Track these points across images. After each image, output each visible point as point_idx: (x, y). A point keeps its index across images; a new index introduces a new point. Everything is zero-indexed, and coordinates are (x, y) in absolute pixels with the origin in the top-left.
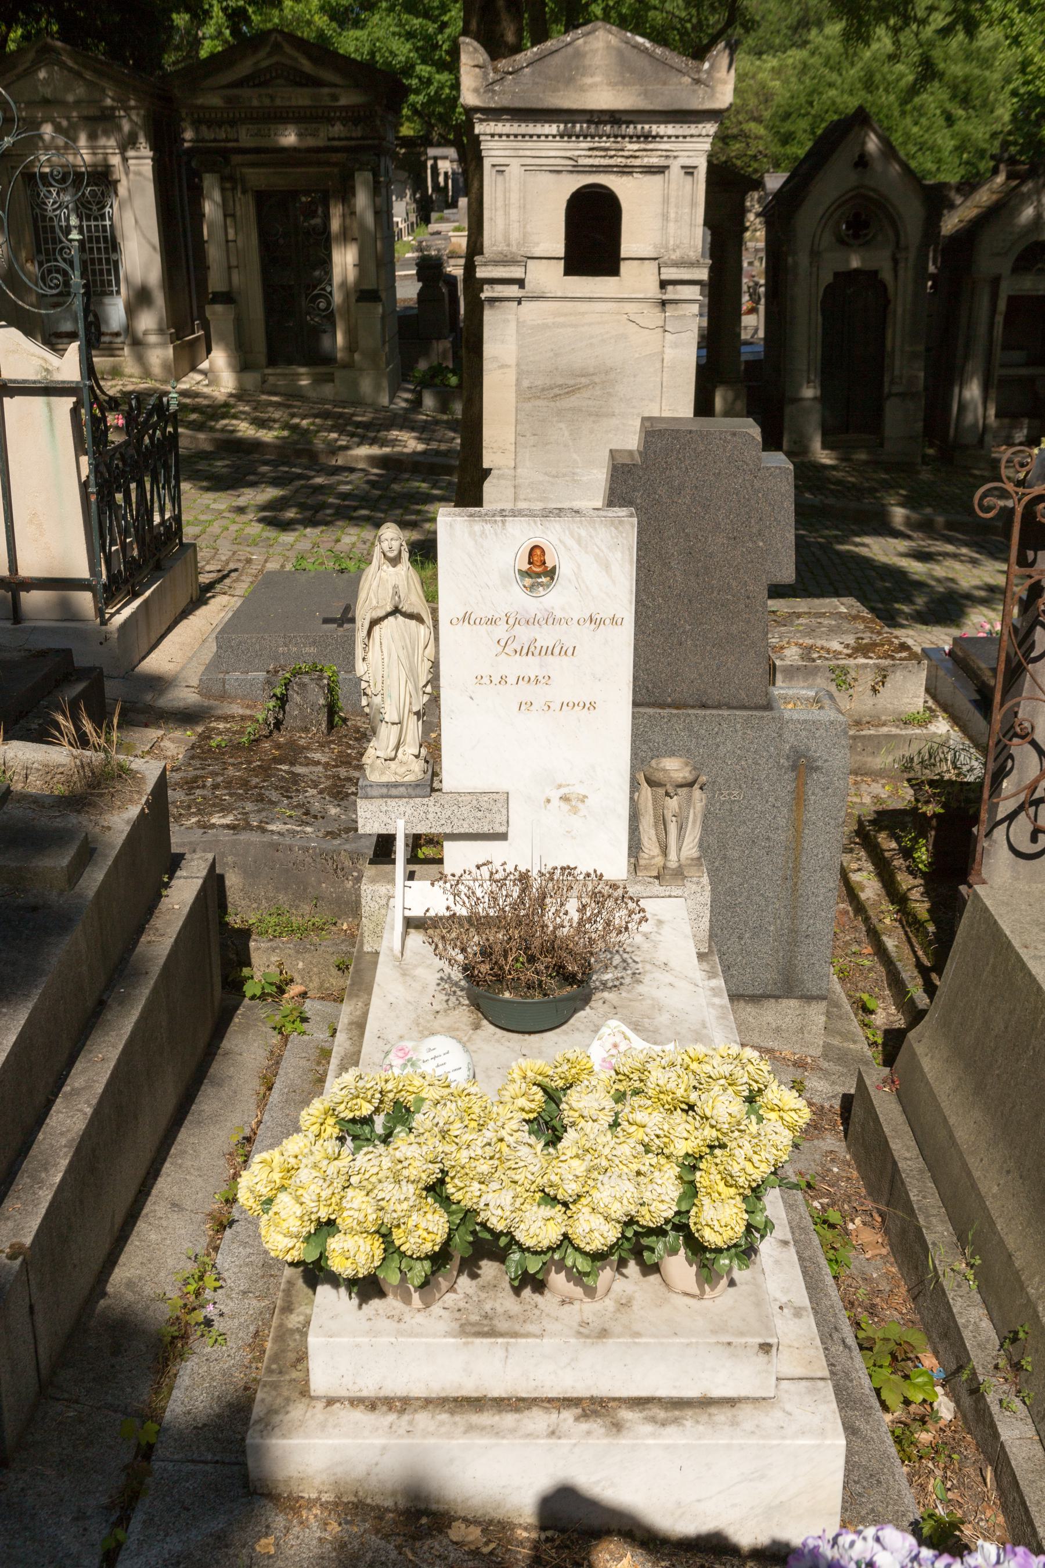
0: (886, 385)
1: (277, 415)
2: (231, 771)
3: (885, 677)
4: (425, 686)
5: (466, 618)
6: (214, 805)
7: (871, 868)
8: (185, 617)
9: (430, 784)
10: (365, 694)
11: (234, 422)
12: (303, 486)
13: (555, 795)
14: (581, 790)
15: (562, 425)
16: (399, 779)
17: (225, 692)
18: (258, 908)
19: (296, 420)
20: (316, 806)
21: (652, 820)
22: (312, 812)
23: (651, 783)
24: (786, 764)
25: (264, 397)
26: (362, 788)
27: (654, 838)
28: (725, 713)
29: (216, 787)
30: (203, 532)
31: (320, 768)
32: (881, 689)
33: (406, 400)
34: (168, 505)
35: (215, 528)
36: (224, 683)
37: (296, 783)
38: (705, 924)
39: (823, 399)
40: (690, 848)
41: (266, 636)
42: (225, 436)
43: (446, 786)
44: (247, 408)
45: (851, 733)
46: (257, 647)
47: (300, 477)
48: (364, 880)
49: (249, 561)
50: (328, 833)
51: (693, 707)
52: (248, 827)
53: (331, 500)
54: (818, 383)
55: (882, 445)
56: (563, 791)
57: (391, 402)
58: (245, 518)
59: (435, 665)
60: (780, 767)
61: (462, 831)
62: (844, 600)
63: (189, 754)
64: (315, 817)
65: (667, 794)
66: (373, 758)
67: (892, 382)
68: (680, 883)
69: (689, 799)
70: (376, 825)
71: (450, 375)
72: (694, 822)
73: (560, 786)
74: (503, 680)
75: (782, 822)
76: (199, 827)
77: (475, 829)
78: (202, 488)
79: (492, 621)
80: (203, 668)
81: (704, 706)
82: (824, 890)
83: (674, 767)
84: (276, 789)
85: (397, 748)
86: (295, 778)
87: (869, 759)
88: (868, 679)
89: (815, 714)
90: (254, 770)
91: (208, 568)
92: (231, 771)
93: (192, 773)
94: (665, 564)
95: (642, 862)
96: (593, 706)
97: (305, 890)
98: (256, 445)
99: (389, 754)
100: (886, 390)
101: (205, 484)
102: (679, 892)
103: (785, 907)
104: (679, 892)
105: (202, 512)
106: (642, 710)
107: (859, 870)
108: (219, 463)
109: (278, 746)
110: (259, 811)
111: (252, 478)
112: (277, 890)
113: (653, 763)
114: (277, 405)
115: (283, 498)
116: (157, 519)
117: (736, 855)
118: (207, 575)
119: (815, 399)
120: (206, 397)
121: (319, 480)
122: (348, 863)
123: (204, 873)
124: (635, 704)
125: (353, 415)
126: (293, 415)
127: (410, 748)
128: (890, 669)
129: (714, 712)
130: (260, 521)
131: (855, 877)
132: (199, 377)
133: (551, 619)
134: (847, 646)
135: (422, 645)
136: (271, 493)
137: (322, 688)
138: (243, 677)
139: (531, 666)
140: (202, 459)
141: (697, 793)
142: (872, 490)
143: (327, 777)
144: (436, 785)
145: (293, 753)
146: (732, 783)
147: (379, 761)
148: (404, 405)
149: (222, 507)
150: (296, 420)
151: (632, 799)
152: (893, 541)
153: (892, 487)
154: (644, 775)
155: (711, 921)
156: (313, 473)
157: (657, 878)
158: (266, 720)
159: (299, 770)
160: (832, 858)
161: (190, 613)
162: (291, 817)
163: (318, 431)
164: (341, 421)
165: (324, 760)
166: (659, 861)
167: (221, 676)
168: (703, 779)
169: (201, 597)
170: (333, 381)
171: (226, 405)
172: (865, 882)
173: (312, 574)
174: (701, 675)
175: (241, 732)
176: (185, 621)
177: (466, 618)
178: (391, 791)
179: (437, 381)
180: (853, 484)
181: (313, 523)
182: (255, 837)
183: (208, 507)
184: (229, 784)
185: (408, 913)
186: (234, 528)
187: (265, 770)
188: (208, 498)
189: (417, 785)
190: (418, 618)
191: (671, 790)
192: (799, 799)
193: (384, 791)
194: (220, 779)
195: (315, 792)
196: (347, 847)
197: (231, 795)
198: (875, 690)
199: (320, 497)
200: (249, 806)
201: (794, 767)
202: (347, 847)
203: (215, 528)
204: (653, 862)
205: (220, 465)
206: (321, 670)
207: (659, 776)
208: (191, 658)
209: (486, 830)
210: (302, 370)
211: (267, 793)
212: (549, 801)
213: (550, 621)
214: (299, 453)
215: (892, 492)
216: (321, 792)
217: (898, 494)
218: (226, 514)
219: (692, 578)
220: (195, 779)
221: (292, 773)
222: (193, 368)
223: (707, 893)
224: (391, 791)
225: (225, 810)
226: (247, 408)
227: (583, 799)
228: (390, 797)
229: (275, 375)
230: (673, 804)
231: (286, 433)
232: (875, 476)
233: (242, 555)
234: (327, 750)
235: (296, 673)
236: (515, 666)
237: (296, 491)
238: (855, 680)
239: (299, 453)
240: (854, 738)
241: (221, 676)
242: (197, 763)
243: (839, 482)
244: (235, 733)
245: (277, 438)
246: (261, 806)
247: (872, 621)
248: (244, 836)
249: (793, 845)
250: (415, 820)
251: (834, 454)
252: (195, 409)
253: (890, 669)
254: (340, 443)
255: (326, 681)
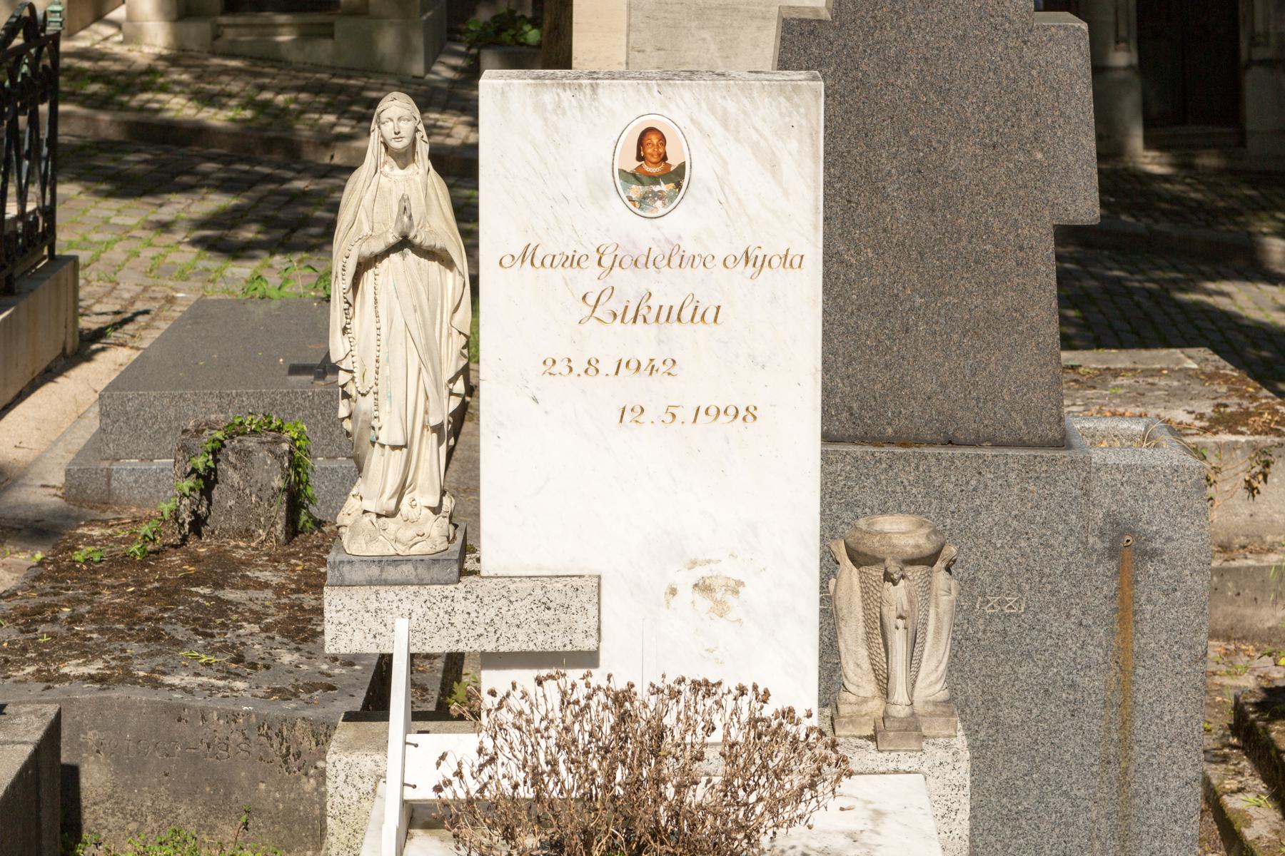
0: (1244, 44)
1: (235, 87)
2: (106, 596)
3: (1267, 465)
4: (453, 380)
5: (527, 256)
6: (70, 647)
7: (1261, 786)
8: (51, 380)
9: (461, 558)
10: (346, 396)
11: (162, 96)
12: (272, 193)
13: (684, 580)
14: (731, 570)
15: (706, 34)
16: (402, 550)
17: (110, 493)
18: (138, 832)
19: (267, 95)
20: (256, 650)
21: (861, 630)
22: (248, 658)
23: (859, 558)
24: (1099, 546)
25: (216, 61)
26: (335, 566)
27: (866, 665)
28: (989, 453)
29: (75, 619)
30: (96, 259)
31: (269, 594)
32: (1261, 486)
33: (454, 68)
34: (34, 190)
35: (117, 253)
36: (109, 477)
37: (222, 614)
38: (962, 824)
39: (1144, 67)
40: (931, 682)
41: (188, 394)
42: (144, 116)
43: (487, 567)
44: (185, 77)
45: (1215, 564)
46: (172, 413)
47: (267, 178)
48: (333, 746)
49: (171, 300)
50: (275, 691)
51: (931, 444)
52: (128, 678)
53: (318, 214)
54: (1133, 44)
55: (1242, 143)
56: (700, 572)
57: (428, 70)
58: (168, 239)
59: (471, 345)
60: (1089, 551)
61: (515, 647)
62: (1192, 351)
63: (33, 573)
64: (253, 666)
65: (888, 577)
66: (356, 513)
67: (1253, 43)
68: (914, 745)
69: (927, 588)
70: (358, 636)
71: (527, 28)
72: (938, 632)
73: (694, 564)
74: (592, 366)
75: (1096, 654)
76: (39, 680)
77: (540, 643)
78: (97, 193)
79: (573, 261)
80: (72, 456)
81: (950, 442)
82: (1175, 784)
83: (900, 531)
84: (185, 622)
85: (400, 493)
86: (222, 607)
87: (1249, 611)
88: (1239, 468)
89: (1148, 456)
90: (149, 593)
91: (97, 308)
92: (106, 596)
93: (35, 600)
94: (875, 191)
95: (845, 710)
96: (751, 414)
97: (227, 796)
98: (198, 132)
99: (385, 509)
100: (1244, 56)
101: (104, 187)
102: (912, 763)
103: (1108, 816)
104: (912, 763)
105: (97, 229)
106: (842, 448)
107: (1240, 790)
108: (131, 158)
109: (196, 560)
110: (151, 655)
111: (185, 179)
112: (177, 796)
113: (862, 523)
114: (235, 73)
115: (236, 209)
116: (12, 210)
117: (1017, 717)
118: (94, 318)
119: (1129, 67)
120: (116, 58)
121: (300, 184)
122: (308, 744)
123: (38, 736)
124: (827, 438)
125: (363, 88)
126: (262, 88)
127: (425, 494)
128: (1275, 452)
129: (970, 451)
130: (194, 243)
131: (1233, 803)
132: (107, 31)
133: (677, 258)
134: (1201, 417)
135: (449, 307)
136: (217, 202)
137: (278, 457)
138: (144, 466)
139: (642, 341)
140: (102, 150)
141: (940, 577)
142: (1231, 213)
143: (280, 608)
144: (469, 565)
145: (222, 570)
146: (1006, 581)
147: (366, 519)
148: (448, 74)
149: (131, 221)
150: (267, 95)
151: (823, 588)
152: (1268, 289)
153: (1264, 209)
154: (846, 548)
155: (973, 817)
156: (290, 174)
157: (873, 738)
158: (176, 515)
159: (228, 594)
160: (1187, 720)
161: (60, 374)
162: (208, 664)
163: (303, 112)
164: (342, 98)
165: (275, 581)
166: (876, 706)
167: (106, 464)
168: (950, 551)
169: (82, 348)
170: (332, 36)
171: (150, 71)
172: (1252, 811)
173: (274, 305)
174: (943, 386)
175: (129, 541)
176: (50, 386)
177: (527, 256)
178: (386, 572)
179: (506, 37)
180: (1199, 202)
181: (283, 246)
182: (139, 695)
183: (106, 222)
184: (100, 616)
185: (410, 795)
186: (148, 253)
187: (169, 594)
188: (111, 209)
189: (434, 561)
190: (444, 259)
191: (893, 568)
192: (1125, 611)
193: (374, 571)
194: (84, 609)
195: (256, 628)
196: (308, 713)
197: (101, 631)
198: (1251, 489)
199: (301, 209)
200: (133, 648)
201: (1113, 552)
202: (308, 713)
203: (117, 253)
204: (865, 709)
205: (134, 161)
206: (279, 429)
207: (871, 545)
208: (55, 443)
209: (558, 645)
210: (282, 18)
211: (168, 628)
212: (673, 592)
213: (676, 260)
214: (269, 145)
215: (1263, 215)
216: (267, 629)
217: (1273, 218)
218: (134, 233)
219: (924, 215)
220: (40, 610)
221: (218, 599)
222: (99, 17)
223: (965, 766)
224: (386, 572)
225: (86, 652)
226: (185, 77)
227: (735, 588)
228: (386, 583)
229: (236, 28)
230: (898, 595)
231: (248, 114)
232: (1234, 192)
233: (159, 291)
234: (282, 566)
235: (236, 431)
236: (614, 341)
237: (261, 200)
238: (1217, 470)
239: (269, 145)
240: (1221, 572)
241: (106, 464)
242: (46, 586)
243: (1176, 199)
244: (120, 541)
245: (233, 120)
246: (154, 647)
247: (1242, 381)
248: (118, 693)
249: (1118, 698)
250: (430, 628)
251: (1165, 158)
252: (96, 77)
253: (1275, 452)
254: (339, 129)
255: (286, 447)
